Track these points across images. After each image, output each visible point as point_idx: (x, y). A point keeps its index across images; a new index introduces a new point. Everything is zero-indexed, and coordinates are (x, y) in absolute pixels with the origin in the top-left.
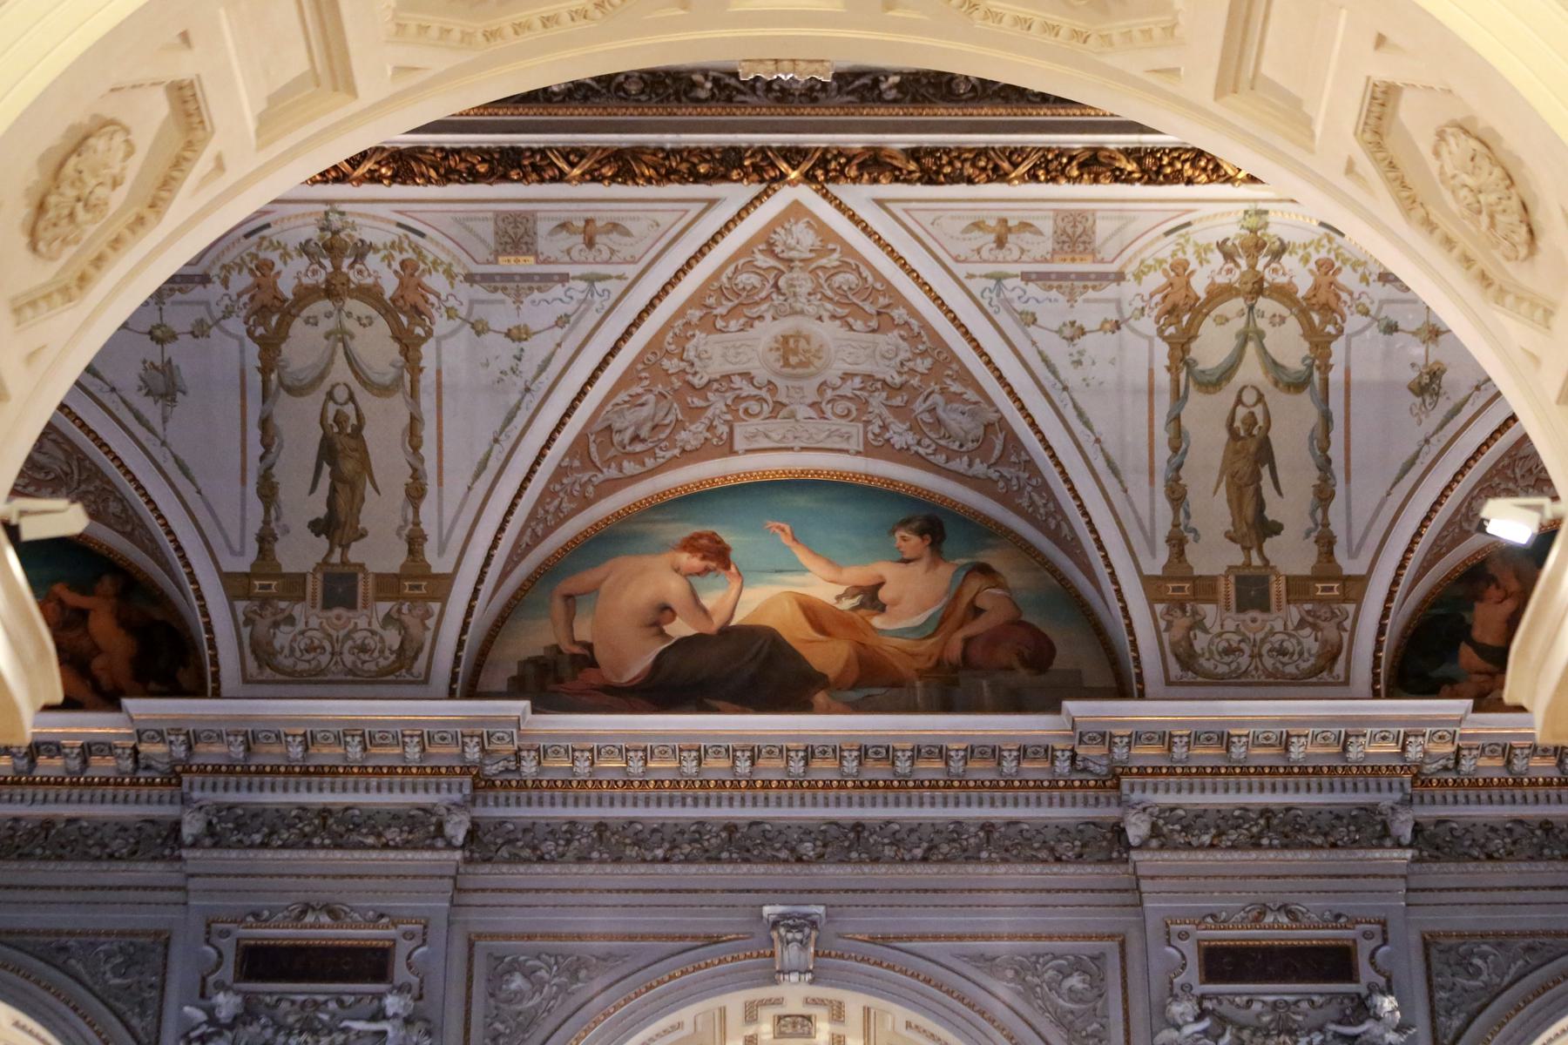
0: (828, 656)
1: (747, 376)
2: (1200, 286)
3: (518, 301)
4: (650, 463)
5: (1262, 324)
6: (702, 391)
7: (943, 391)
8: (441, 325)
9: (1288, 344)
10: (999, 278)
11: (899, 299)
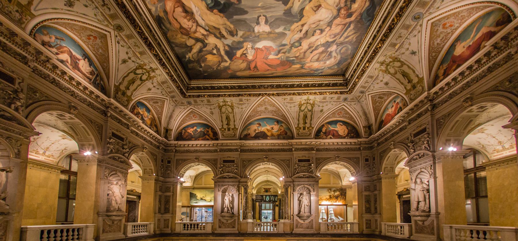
0: (269, 134)
8: (235, 108)
9: (310, 108)
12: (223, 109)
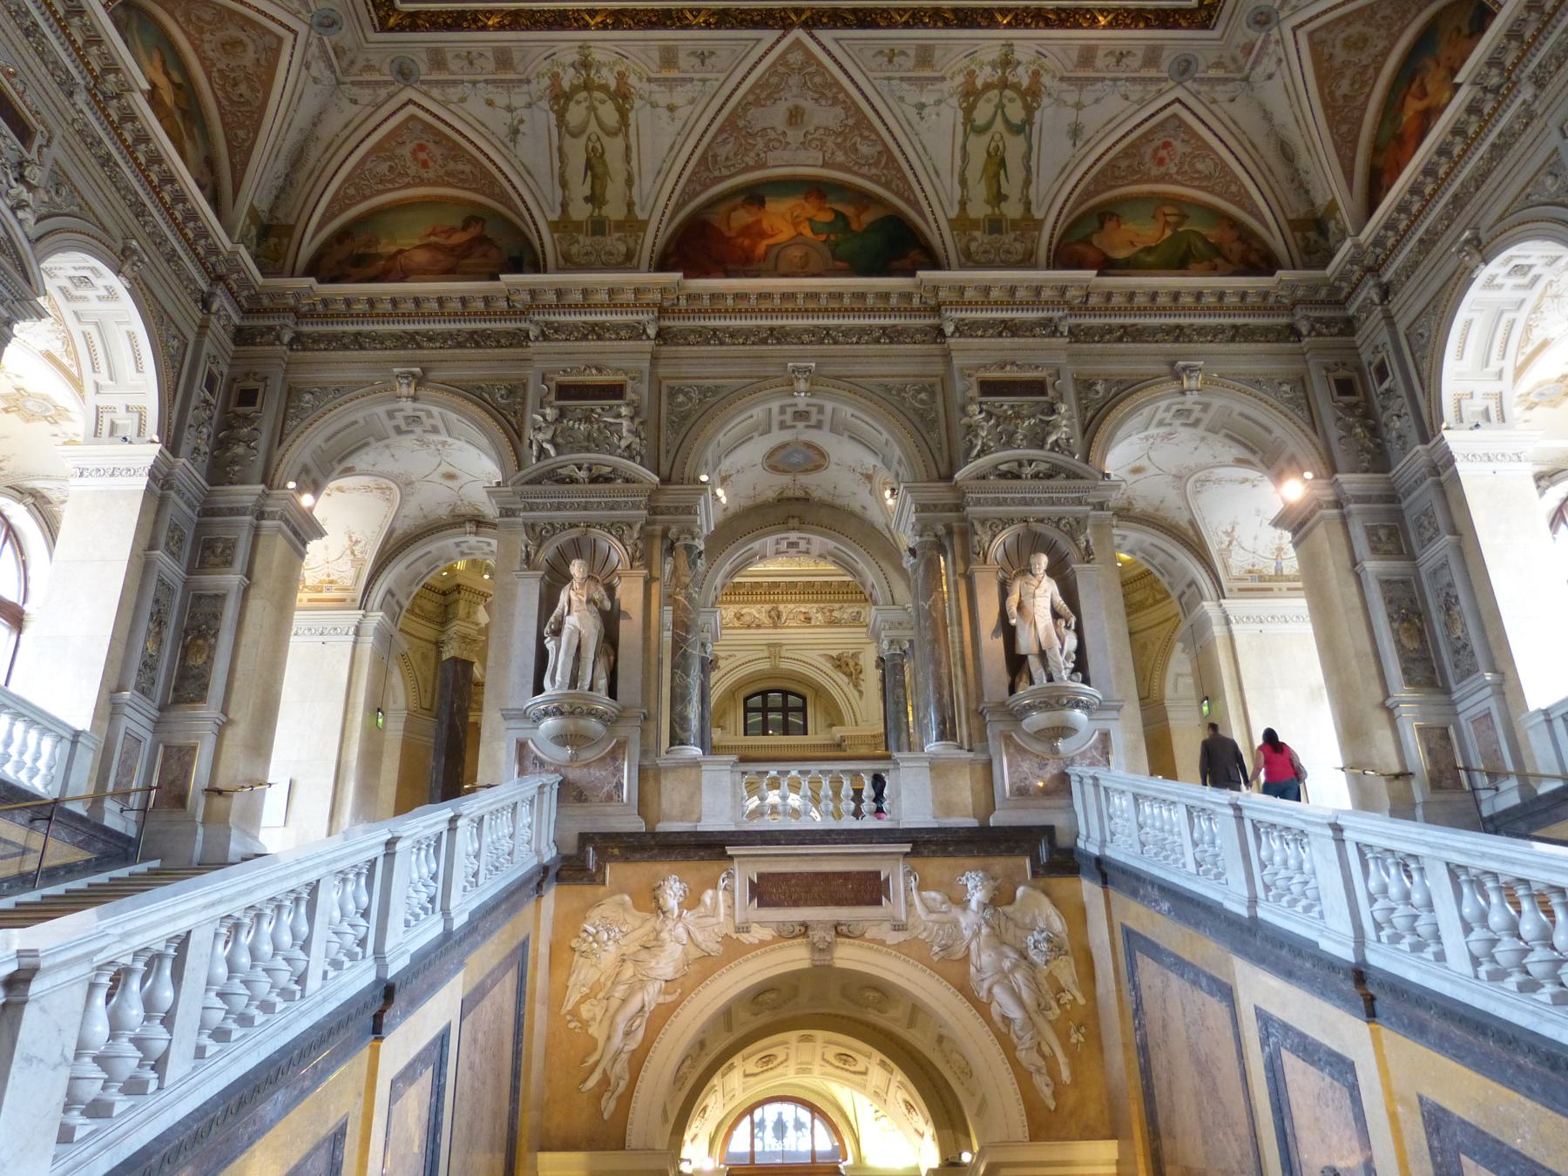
1: (773, 128)
2: (979, 83)
3: (671, 90)
4: (733, 170)
5: (1005, 101)
6: (753, 136)
7: (861, 135)
8: (638, 103)
9: (1016, 113)
10: (889, 79)
11: (842, 89)
12: (576, 114)
